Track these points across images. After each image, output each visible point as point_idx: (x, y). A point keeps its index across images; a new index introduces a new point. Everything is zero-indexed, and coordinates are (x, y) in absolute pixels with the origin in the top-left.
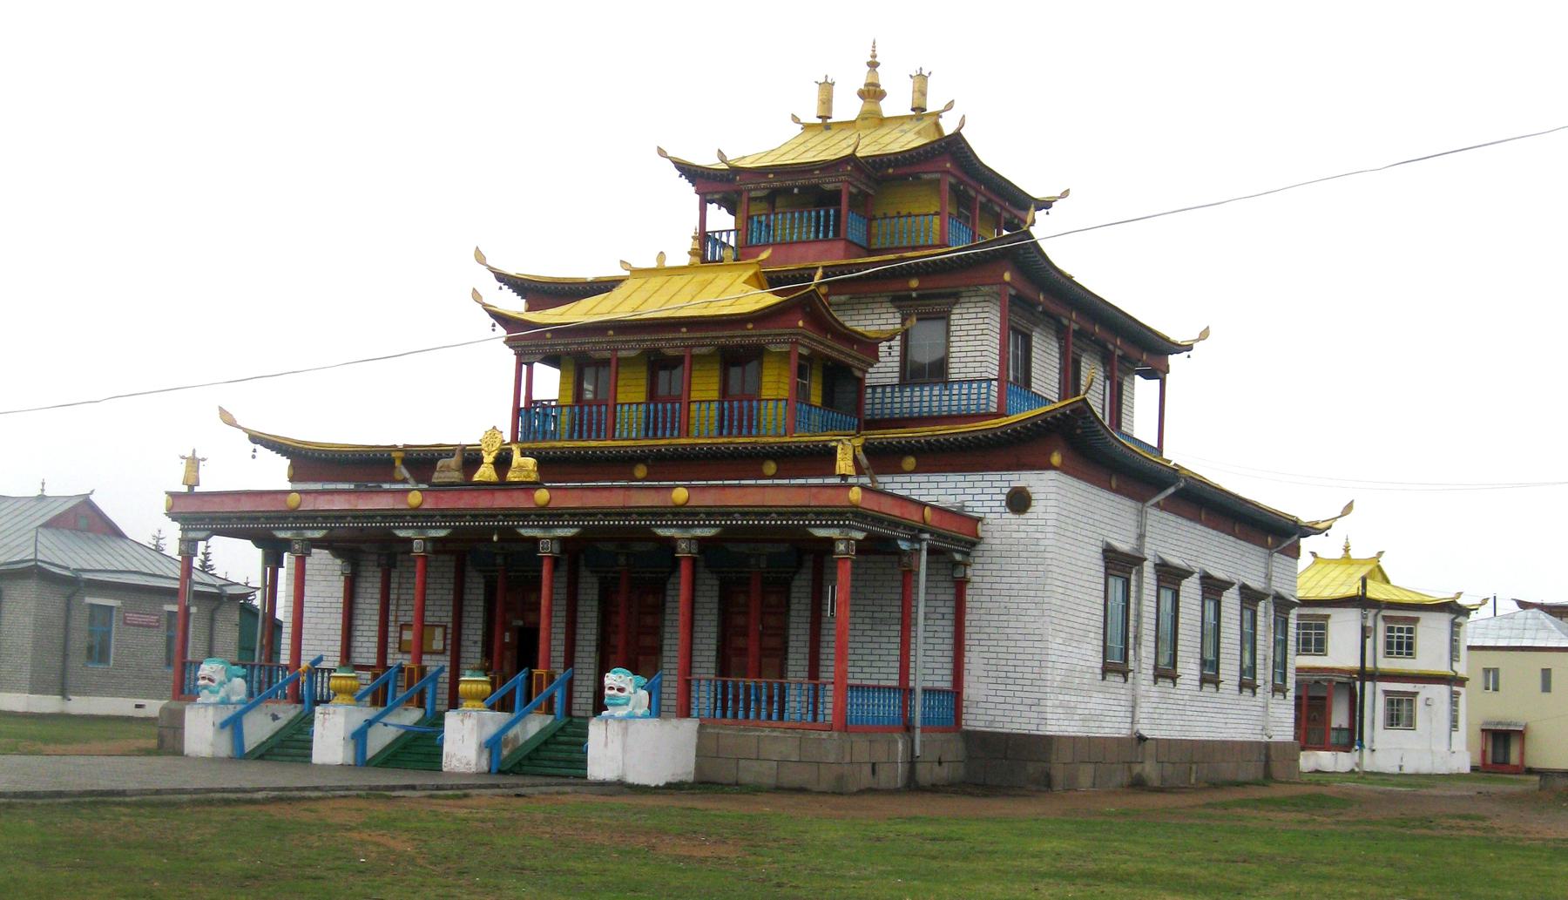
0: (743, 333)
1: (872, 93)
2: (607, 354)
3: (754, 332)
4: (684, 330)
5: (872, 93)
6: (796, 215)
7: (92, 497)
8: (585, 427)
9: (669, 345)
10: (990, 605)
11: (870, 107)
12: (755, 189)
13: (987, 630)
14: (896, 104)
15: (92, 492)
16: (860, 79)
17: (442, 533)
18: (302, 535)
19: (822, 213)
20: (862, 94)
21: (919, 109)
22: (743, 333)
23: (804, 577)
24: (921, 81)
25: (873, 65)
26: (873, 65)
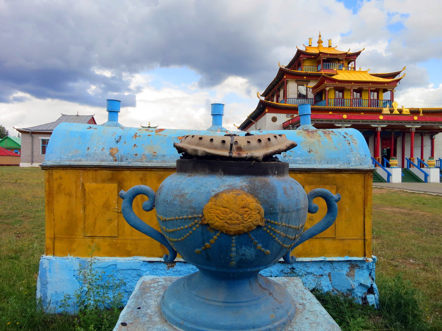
0: (384, 86)
1: (320, 42)
2: (350, 88)
3: (387, 86)
4: (370, 84)
5: (320, 42)
6: (333, 64)
7: (94, 116)
8: (357, 104)
9: (365, 87)
10: (438, 143)
11: (321, 44)
12: (324, 57)
13: (438, 148)
14: (325, 44)
15: (94, 115)
16: (317, 39)
17: (385, 126)
18: (344, 125)
19: (328, 64)
20: (318, 43)
21: (330, 47)
22: (384, 86)
23: (400, 137)
24: (329, 41)
25: (320, 36)
26: (320, 36)
